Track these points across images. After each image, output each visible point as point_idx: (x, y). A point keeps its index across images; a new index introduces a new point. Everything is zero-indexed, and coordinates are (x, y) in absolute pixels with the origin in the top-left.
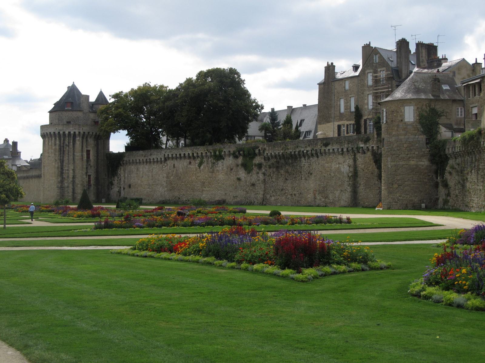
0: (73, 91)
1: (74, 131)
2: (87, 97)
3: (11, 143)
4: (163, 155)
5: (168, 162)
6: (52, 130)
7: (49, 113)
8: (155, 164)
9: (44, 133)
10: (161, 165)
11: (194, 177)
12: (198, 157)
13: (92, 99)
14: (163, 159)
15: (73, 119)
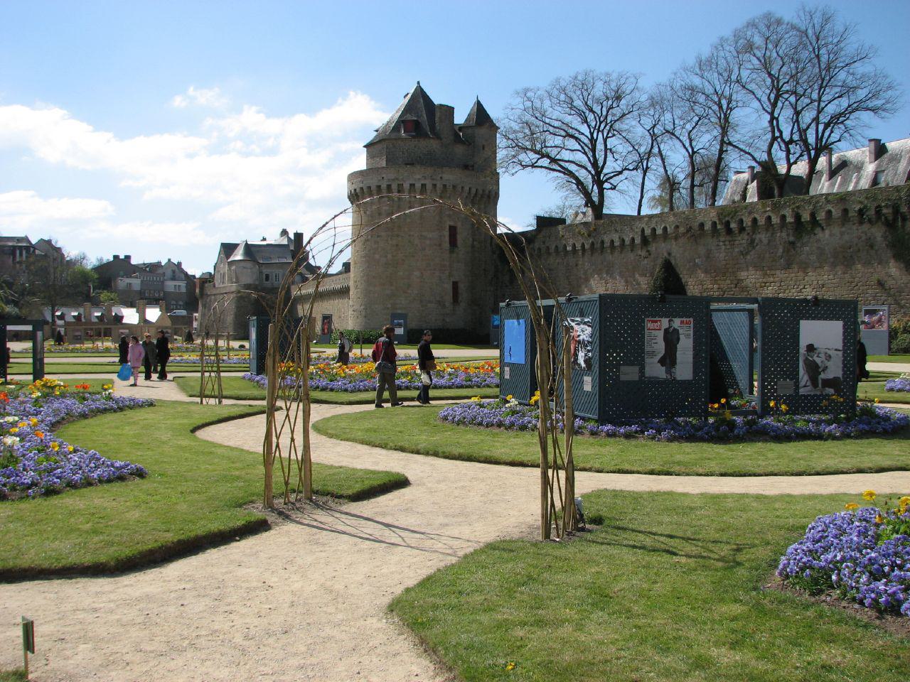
0: (420, 98)
1: (423, 182)
2: (449, 111)
3: (292, 236)
4: (639, 231)
5: (653, 247)
6: (373, 182)
7: (365, 149)
8: (616, 254)
9: (355, 190)
10: (632, 256)
11: (729, 282)
12: (742, 229)
13: (460, 118)
14: (638, 241)
15: (420, 157)
